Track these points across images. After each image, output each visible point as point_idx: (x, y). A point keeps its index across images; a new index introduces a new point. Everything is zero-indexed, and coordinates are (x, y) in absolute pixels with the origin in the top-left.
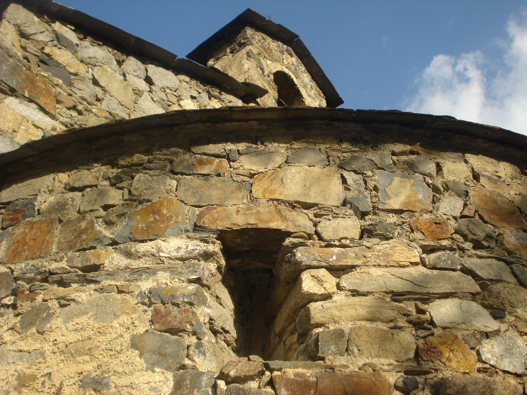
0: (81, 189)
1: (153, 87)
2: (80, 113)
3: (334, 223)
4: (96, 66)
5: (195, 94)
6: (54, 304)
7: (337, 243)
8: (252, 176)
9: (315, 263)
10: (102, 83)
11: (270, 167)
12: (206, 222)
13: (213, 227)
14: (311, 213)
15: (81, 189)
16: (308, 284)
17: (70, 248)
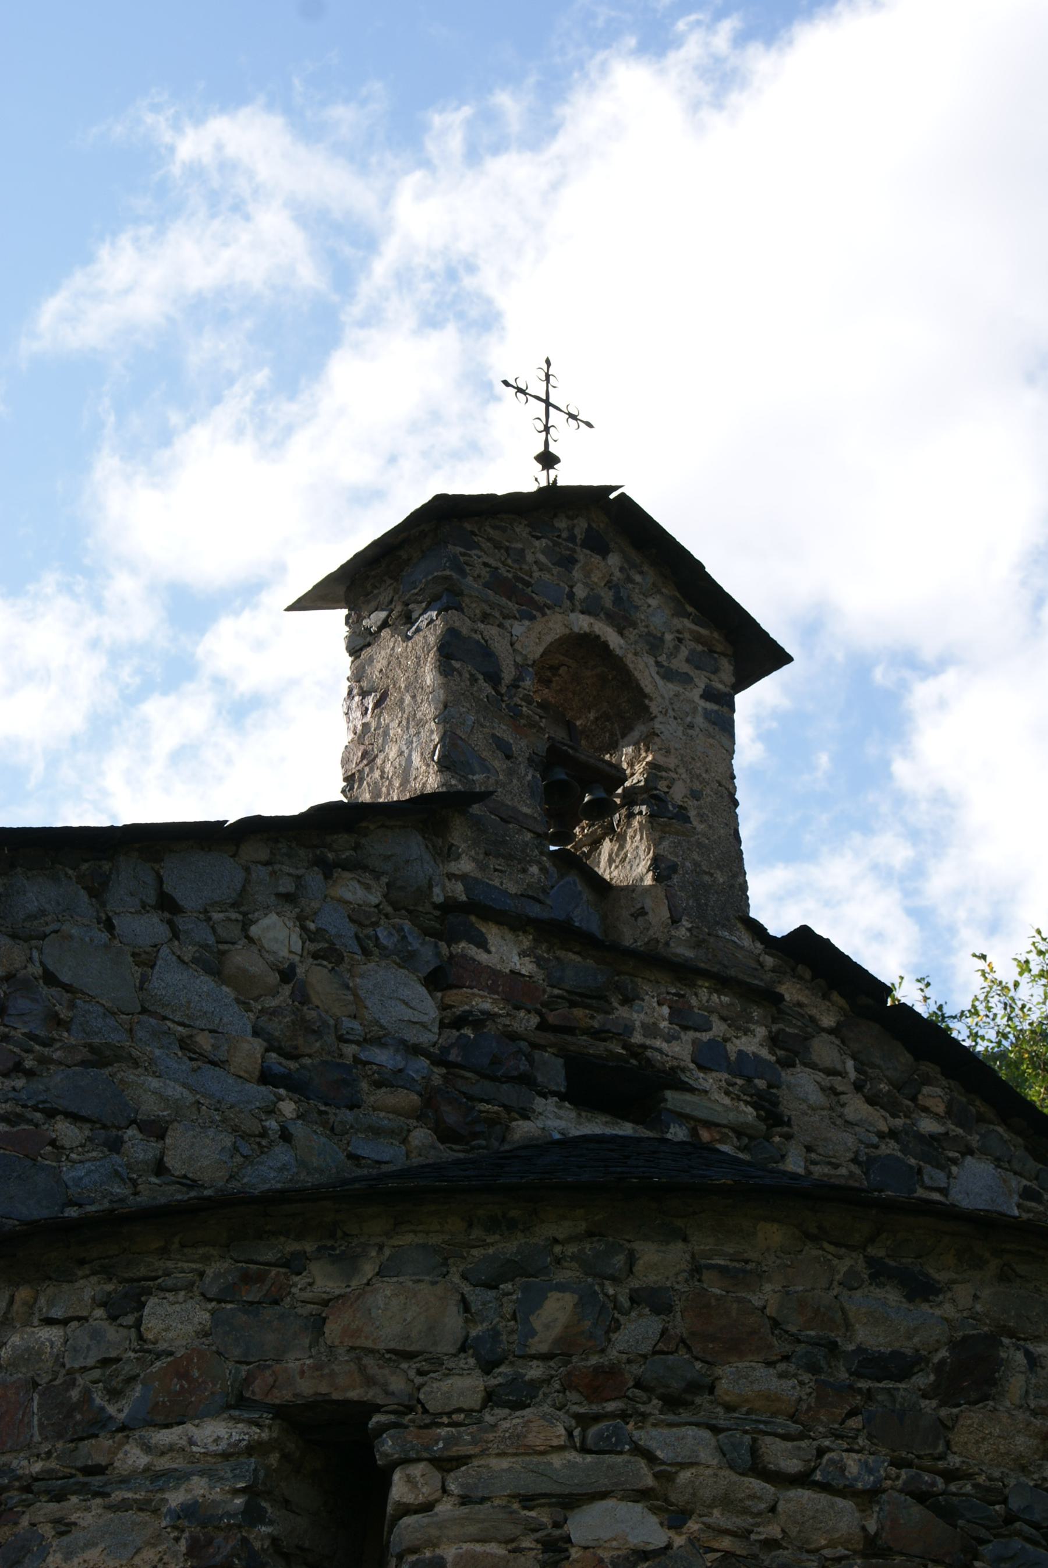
0: (64, 1322)
1: (179, 920)
2: (30, 1074)
3: (445, 1385)
4: (45, 936)
5: (287, 886)
6: (47, 1530)
7: (445, 1420)
8: (325, 1303)
9: (413, 1455)
10: (65, 978)
11: (354, 1283)
12: (257, 1390)
13: (268, 1400)
14: (410, 1368)
15: (64, 1322)
16: (399, 1491)
17: (60, 1436)
